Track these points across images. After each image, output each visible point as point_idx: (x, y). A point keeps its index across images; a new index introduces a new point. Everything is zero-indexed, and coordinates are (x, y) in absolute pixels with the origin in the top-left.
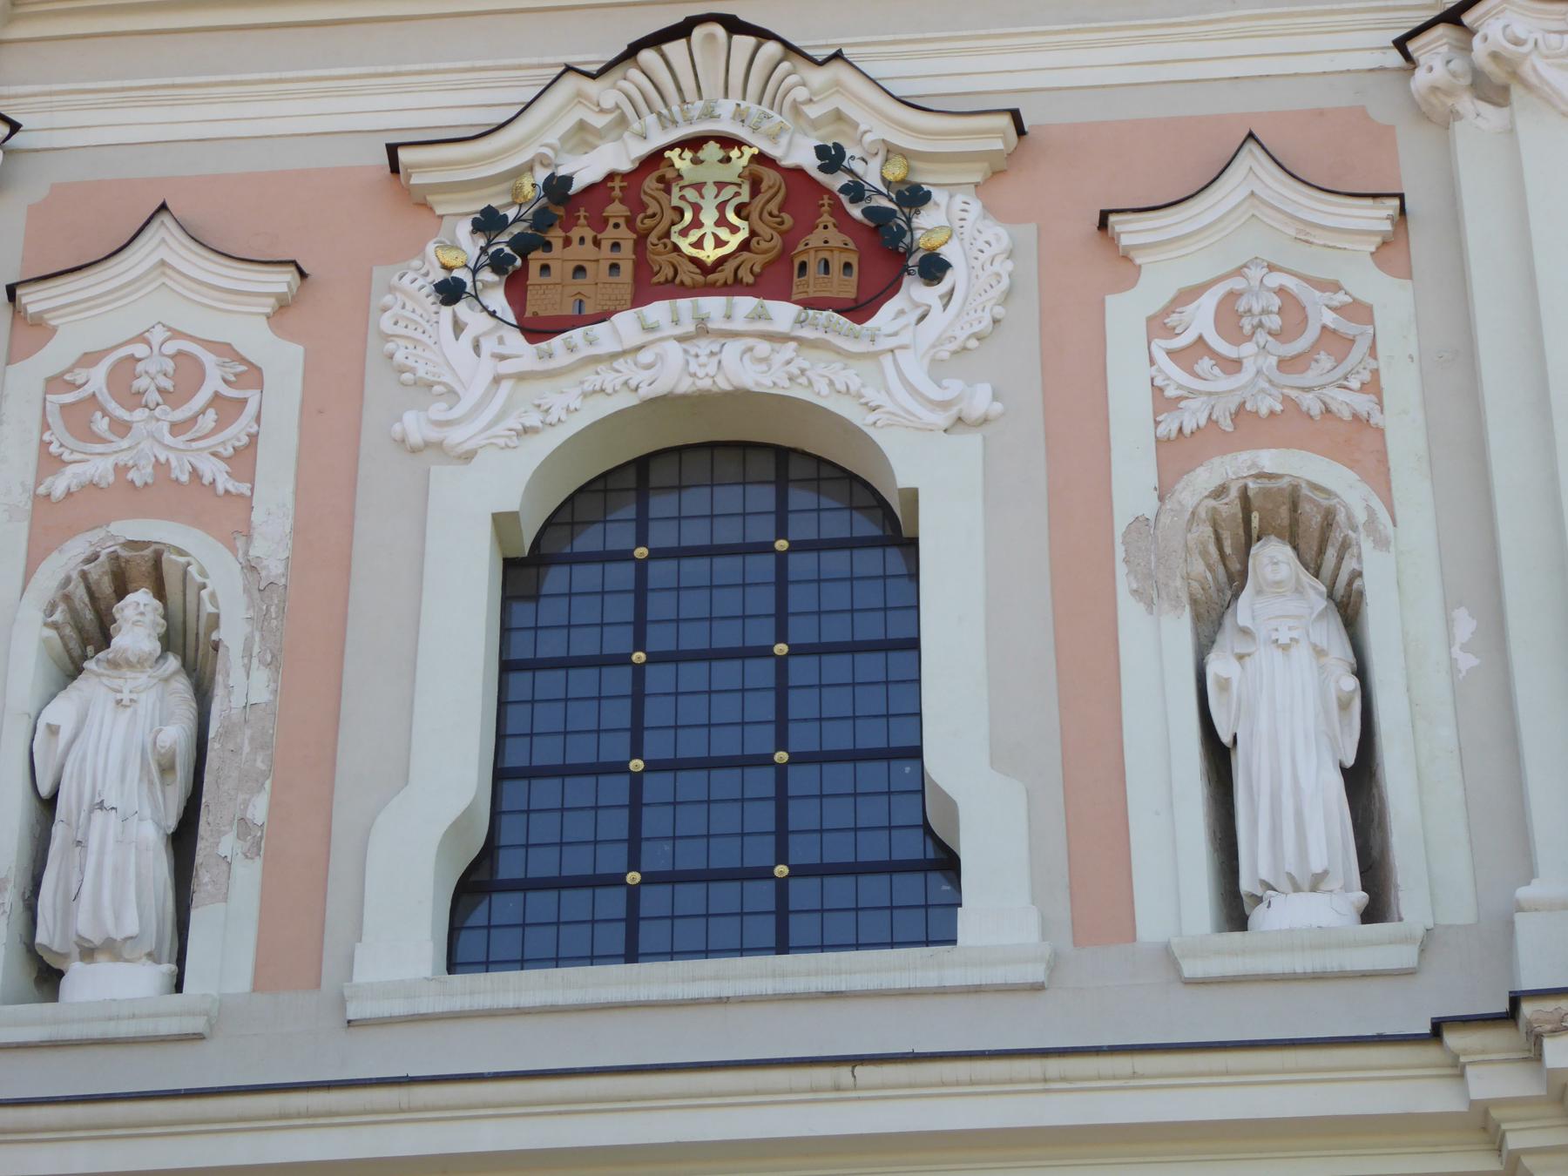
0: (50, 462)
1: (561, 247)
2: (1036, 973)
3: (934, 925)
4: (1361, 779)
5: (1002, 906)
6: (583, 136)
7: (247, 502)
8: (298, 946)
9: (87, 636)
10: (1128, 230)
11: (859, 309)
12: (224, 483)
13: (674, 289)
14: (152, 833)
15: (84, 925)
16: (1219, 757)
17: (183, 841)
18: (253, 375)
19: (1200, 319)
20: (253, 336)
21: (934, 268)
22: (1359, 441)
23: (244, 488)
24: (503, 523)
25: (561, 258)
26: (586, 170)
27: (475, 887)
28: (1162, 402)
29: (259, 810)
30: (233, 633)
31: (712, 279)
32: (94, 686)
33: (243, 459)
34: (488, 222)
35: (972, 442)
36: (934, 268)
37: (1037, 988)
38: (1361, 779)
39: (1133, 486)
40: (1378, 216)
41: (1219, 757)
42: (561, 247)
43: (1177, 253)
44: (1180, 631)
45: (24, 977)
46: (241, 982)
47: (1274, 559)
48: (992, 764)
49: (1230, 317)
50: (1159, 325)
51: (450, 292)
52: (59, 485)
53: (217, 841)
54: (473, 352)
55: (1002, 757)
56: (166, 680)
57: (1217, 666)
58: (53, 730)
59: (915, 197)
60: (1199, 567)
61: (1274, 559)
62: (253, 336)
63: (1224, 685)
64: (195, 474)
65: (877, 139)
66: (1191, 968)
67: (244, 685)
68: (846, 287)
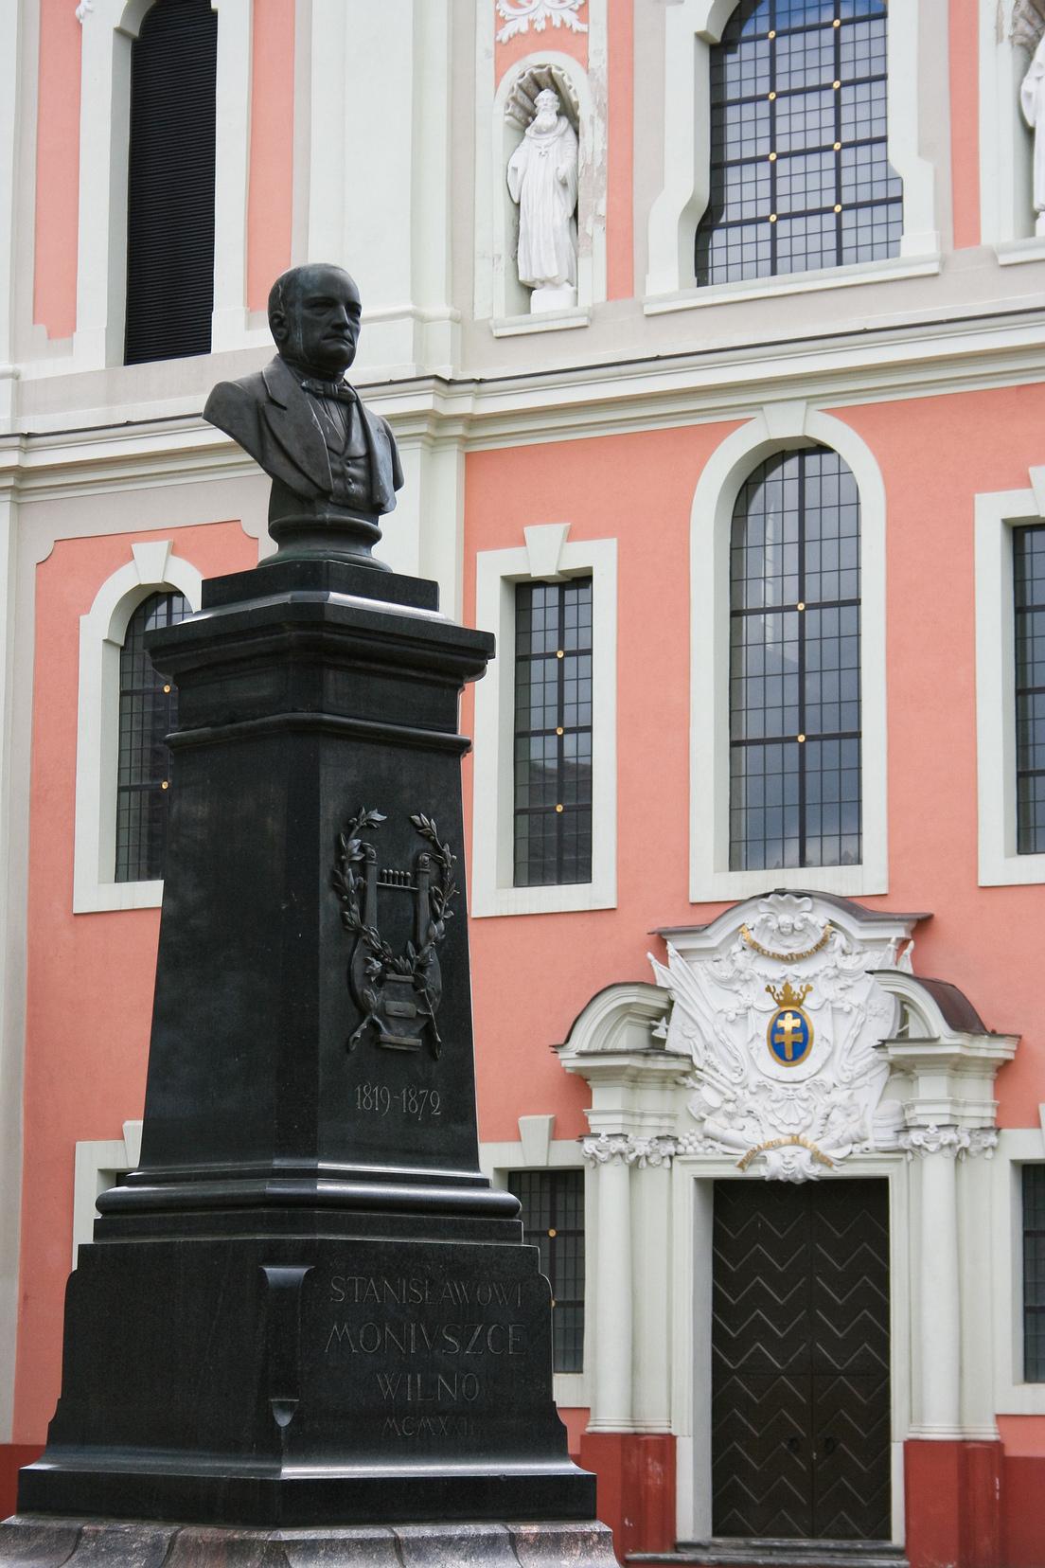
0: (501, 22)
2: (934, 268)
3: (890, 247)
5: (921, 236)
7: (585, 34)
8: (622, 279)
12: (578, 26)
15: (537, 275)
16: (1030, 133)
23: (583, 27)
24: (701, 37)
27: (709, 222)
29: (602, 210)
30: (584, 113)
32: (531, 142)
37: (935, 275)
45: (516, 295)
46: (602, 297)
48: (919, 154)
52: (504, 35)
55: (924, 150)
56: (563, 135)
57: (1029, 85)
58: (515, 169)
60: (1022, 23)
63: (1029, 96)
64: (563, 22)
66: (1003, 260)
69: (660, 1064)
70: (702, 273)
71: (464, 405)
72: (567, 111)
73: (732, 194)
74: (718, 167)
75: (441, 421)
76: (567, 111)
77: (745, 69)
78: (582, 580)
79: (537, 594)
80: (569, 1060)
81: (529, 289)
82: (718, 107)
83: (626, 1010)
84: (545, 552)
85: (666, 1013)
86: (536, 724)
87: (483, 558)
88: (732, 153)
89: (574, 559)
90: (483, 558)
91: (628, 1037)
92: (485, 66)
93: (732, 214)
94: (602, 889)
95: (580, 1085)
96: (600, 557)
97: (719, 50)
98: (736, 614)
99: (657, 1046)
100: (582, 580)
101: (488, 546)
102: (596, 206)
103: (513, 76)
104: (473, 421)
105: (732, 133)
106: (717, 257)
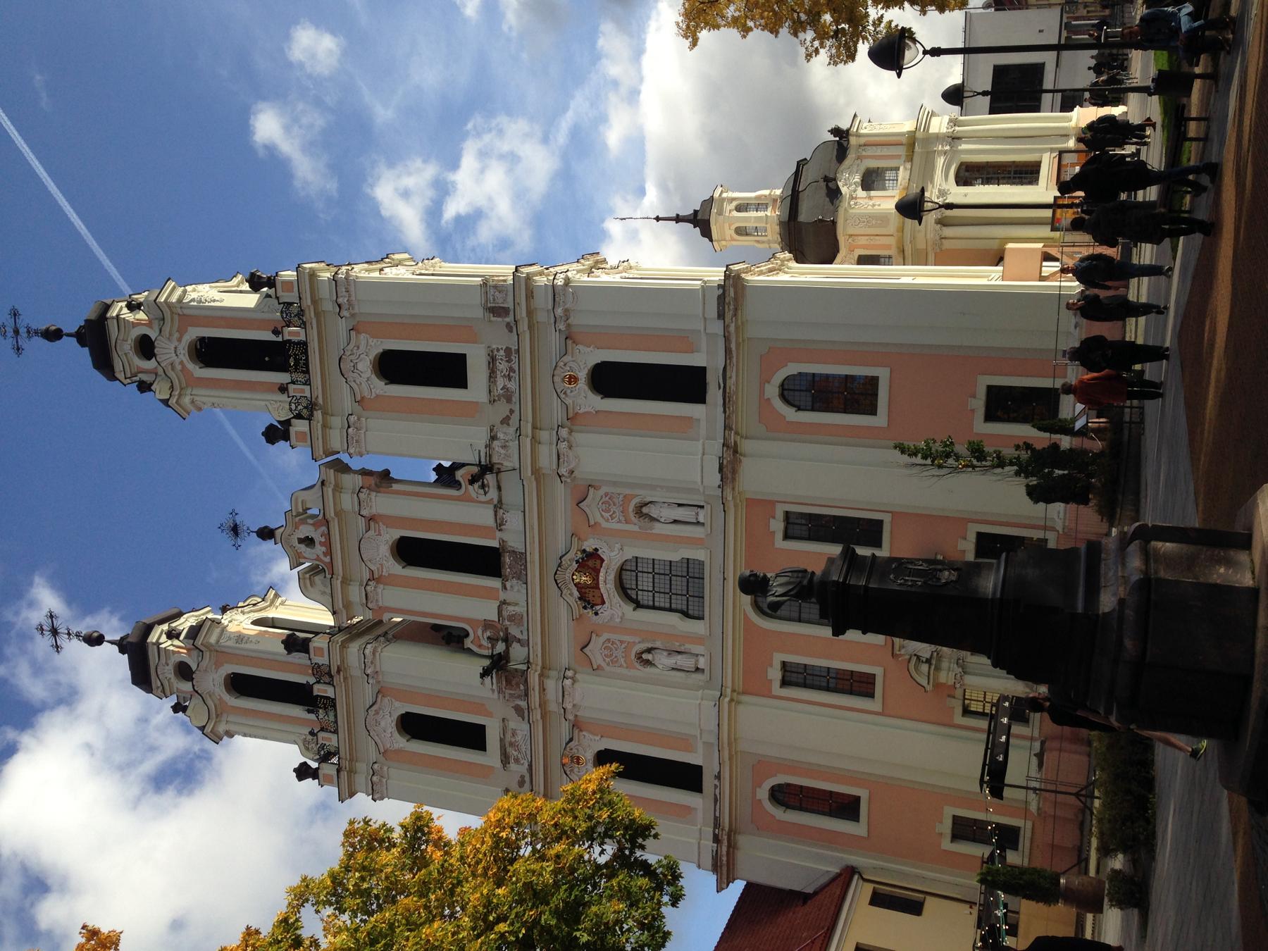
0: (621, 666)
1: (589, 598)
3: (701, 563)
4: (680, 505)
5: (699, 554)
6: (571, 594)
8: (699, 640)
9: (648, 663)
10: (592, 523)
11: (603, 561)
13: (598, 584)
14: (679, 657)
16: (675, 522)
17: (679, 653)
18: (609, 640)
19: (607, 515)
20: (602, 639)
21: (596, 550)
22: (627, 498)
25: (591, 599)
26: (576, 594)
27: (686, 614)
28: (620, 522)
30: (650, 646)
31: (596, 579)
33: (622, 642)
34: (585, 608)
35: (625, 548)
36: (596, 550)
38: (680, 505)
39: (636, 528)
40: (591, 490)
41: (675, 522)
42: (589, 598)
43: (596, 516)
44: (657, 525)
47: (645, 510)
49: (607, 511)
50: (607, 520)
51: (596, 614)
53: (682, 649)
54: (606, 612)
59: (584, 551)
61: (645, 510)
62: (602, 639)
65: (574, 554)
67: (658, 644)
68: (598, 562)
69: (934, 662)
70: (701, 618)
71: (729, 691)
72: (649, 651)
73: (679, 607)
74: (671, 610)
75: (732, 700)
76: (649, 651)
77: (645, 598)
78: (784, 664)
79: (787, 679)
80: (929, 688)
81: (697, 669)
82: (654, 608)
83: (916, 669)
84: (775, 674)
85: (918, 657)
86: (824, 684)
87: (774, 693)
88: (667, 605)
89: (778, 666)
90: (774, 693)
91: (925, 667)
92: (633, 672)
93: (684, 608)
94: (878, 671)
95: (938, 686)
96: (778, 658)
97: (638, 605)
98: (800, 621)
99: (928, 661)
100: (784, 664)
101: (770, 690)
102: (676, 646)
103: (638, 666)
104: (733, 691)
105: (662, 605)
106: (696, 614)
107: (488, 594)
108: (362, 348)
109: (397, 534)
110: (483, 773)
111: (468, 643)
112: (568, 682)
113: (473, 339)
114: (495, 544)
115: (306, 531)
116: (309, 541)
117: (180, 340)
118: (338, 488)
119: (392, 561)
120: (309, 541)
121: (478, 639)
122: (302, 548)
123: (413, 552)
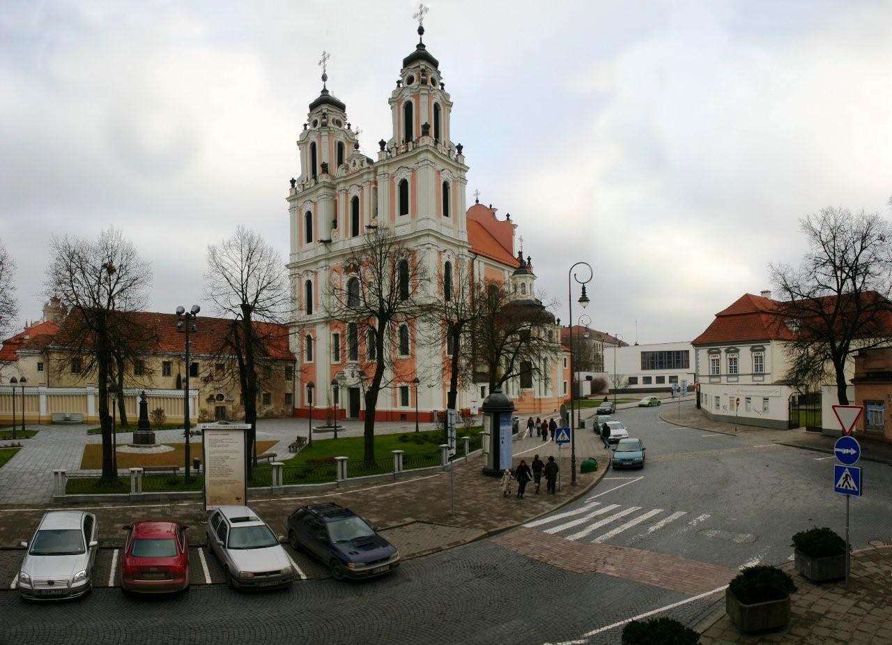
42: (347, 270)
107: (347, 236)
108: (408, 174)
109: (359, 197)
110: (301, 245)
111: (334, 230)
112: (325, 268)
113: (413, 216)
114: (359, 235)
115: (358, 162)
116: (355, 164)
117: (411, 96)
118: (369, 173)
119: (352, 197)
120: (355, 164)
121: (334, 234)
122: (353, 162)
123: (356, 201)
